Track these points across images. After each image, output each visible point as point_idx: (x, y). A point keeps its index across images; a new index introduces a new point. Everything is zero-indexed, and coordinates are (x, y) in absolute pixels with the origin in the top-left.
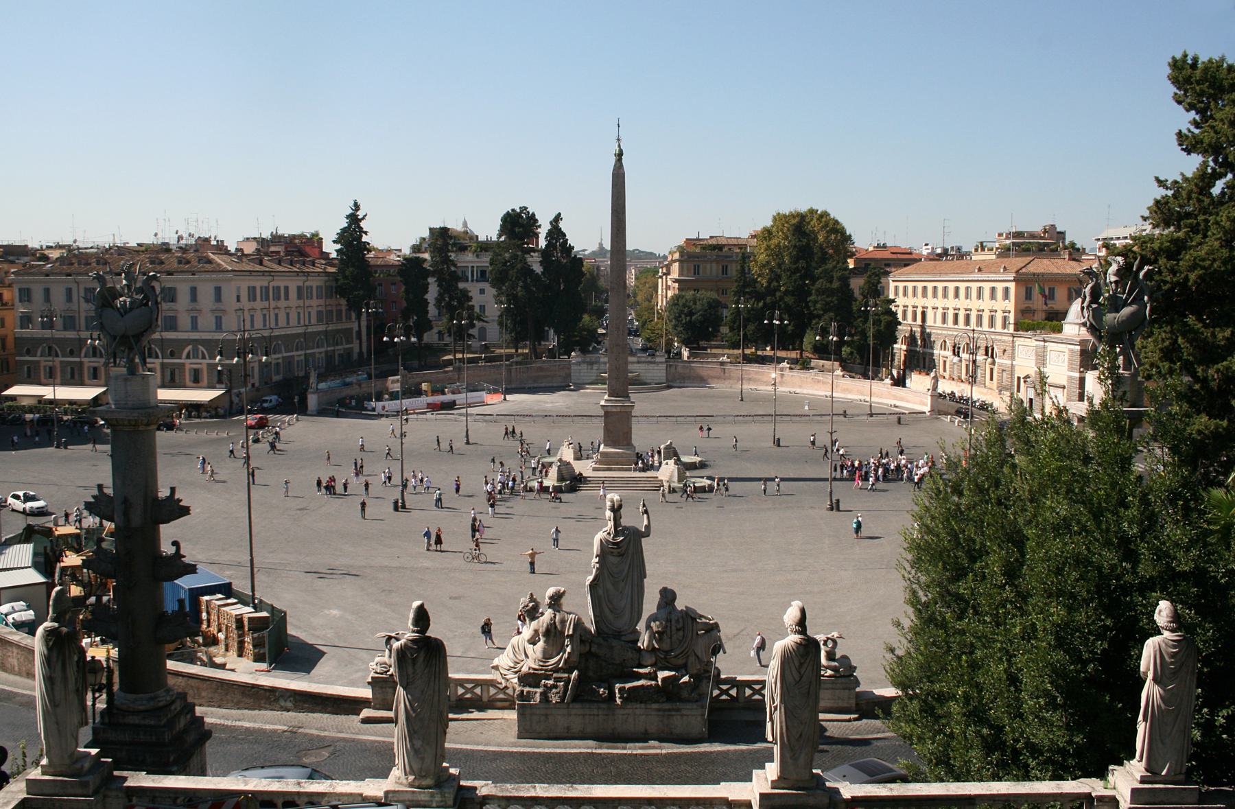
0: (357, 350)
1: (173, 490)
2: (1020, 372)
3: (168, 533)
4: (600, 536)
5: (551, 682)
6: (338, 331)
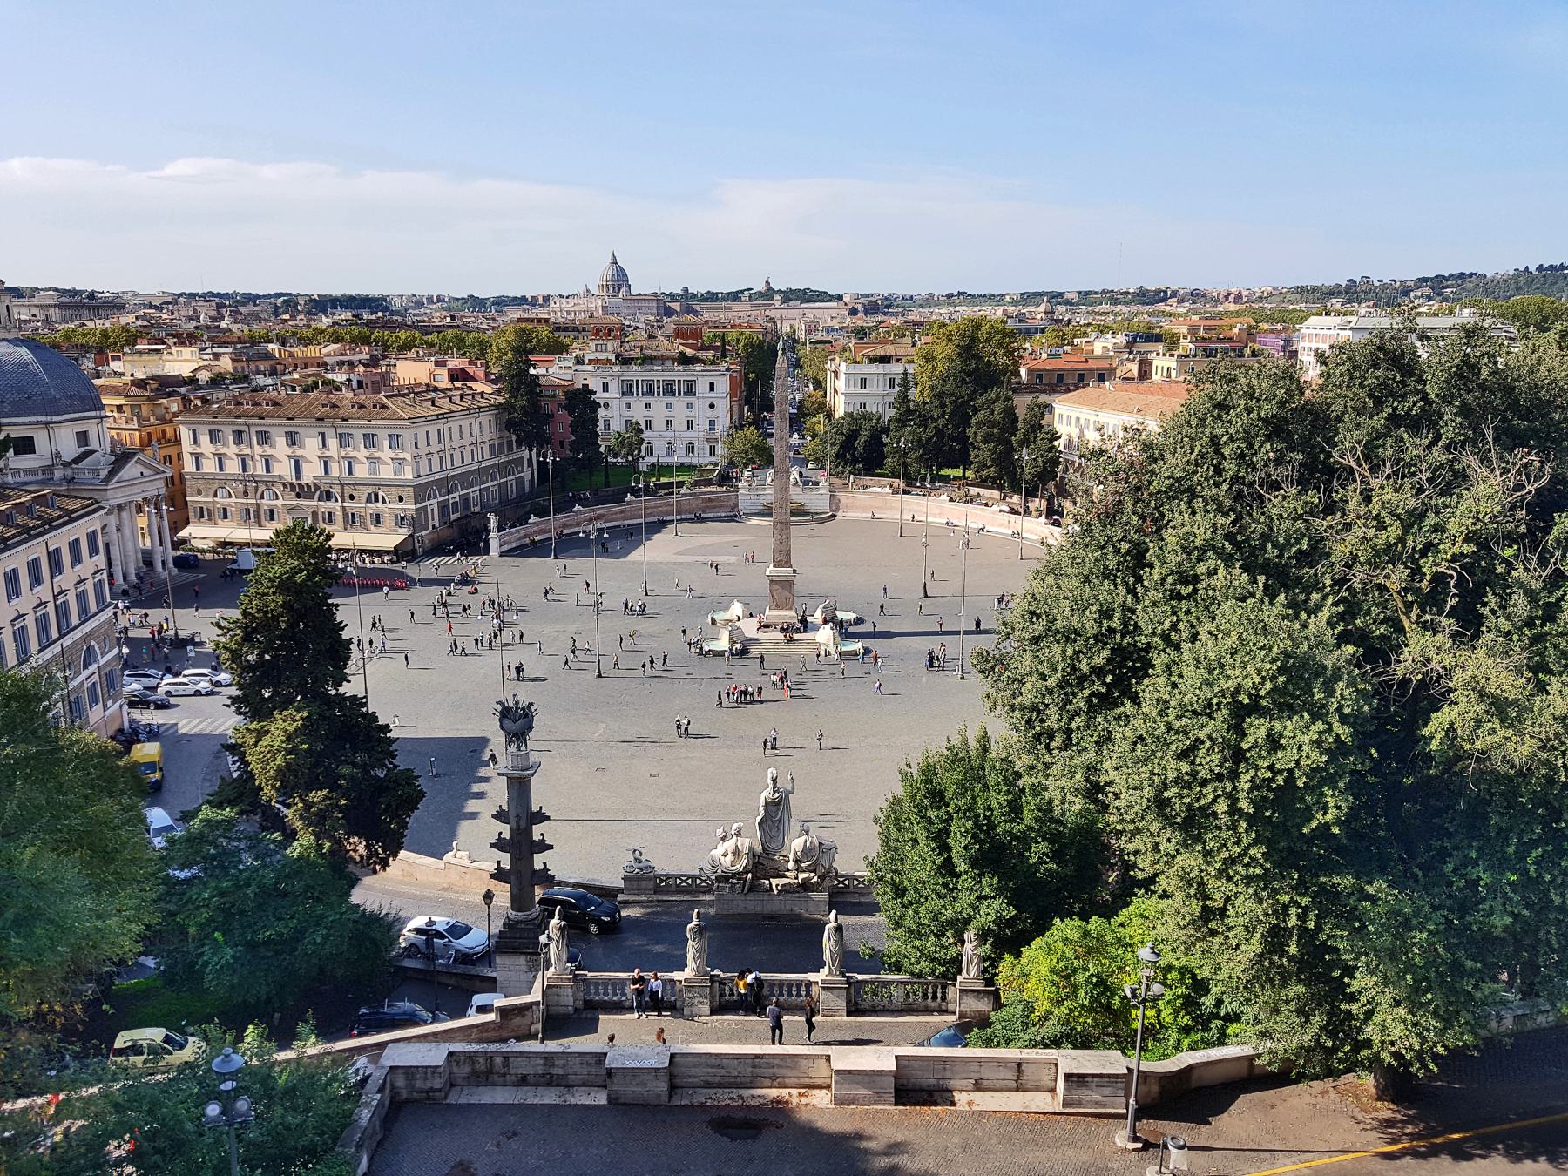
4: (763, 795)
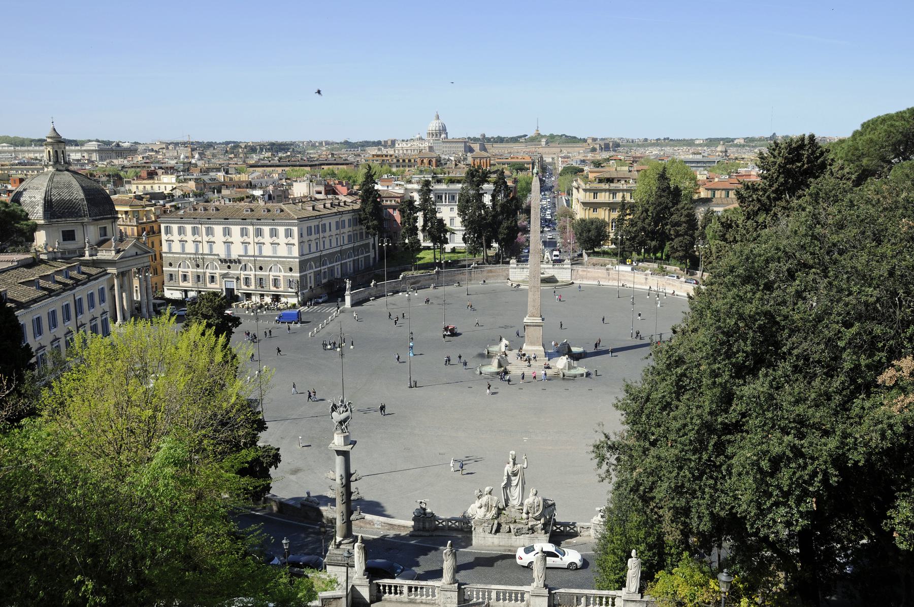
6: (360, 246)
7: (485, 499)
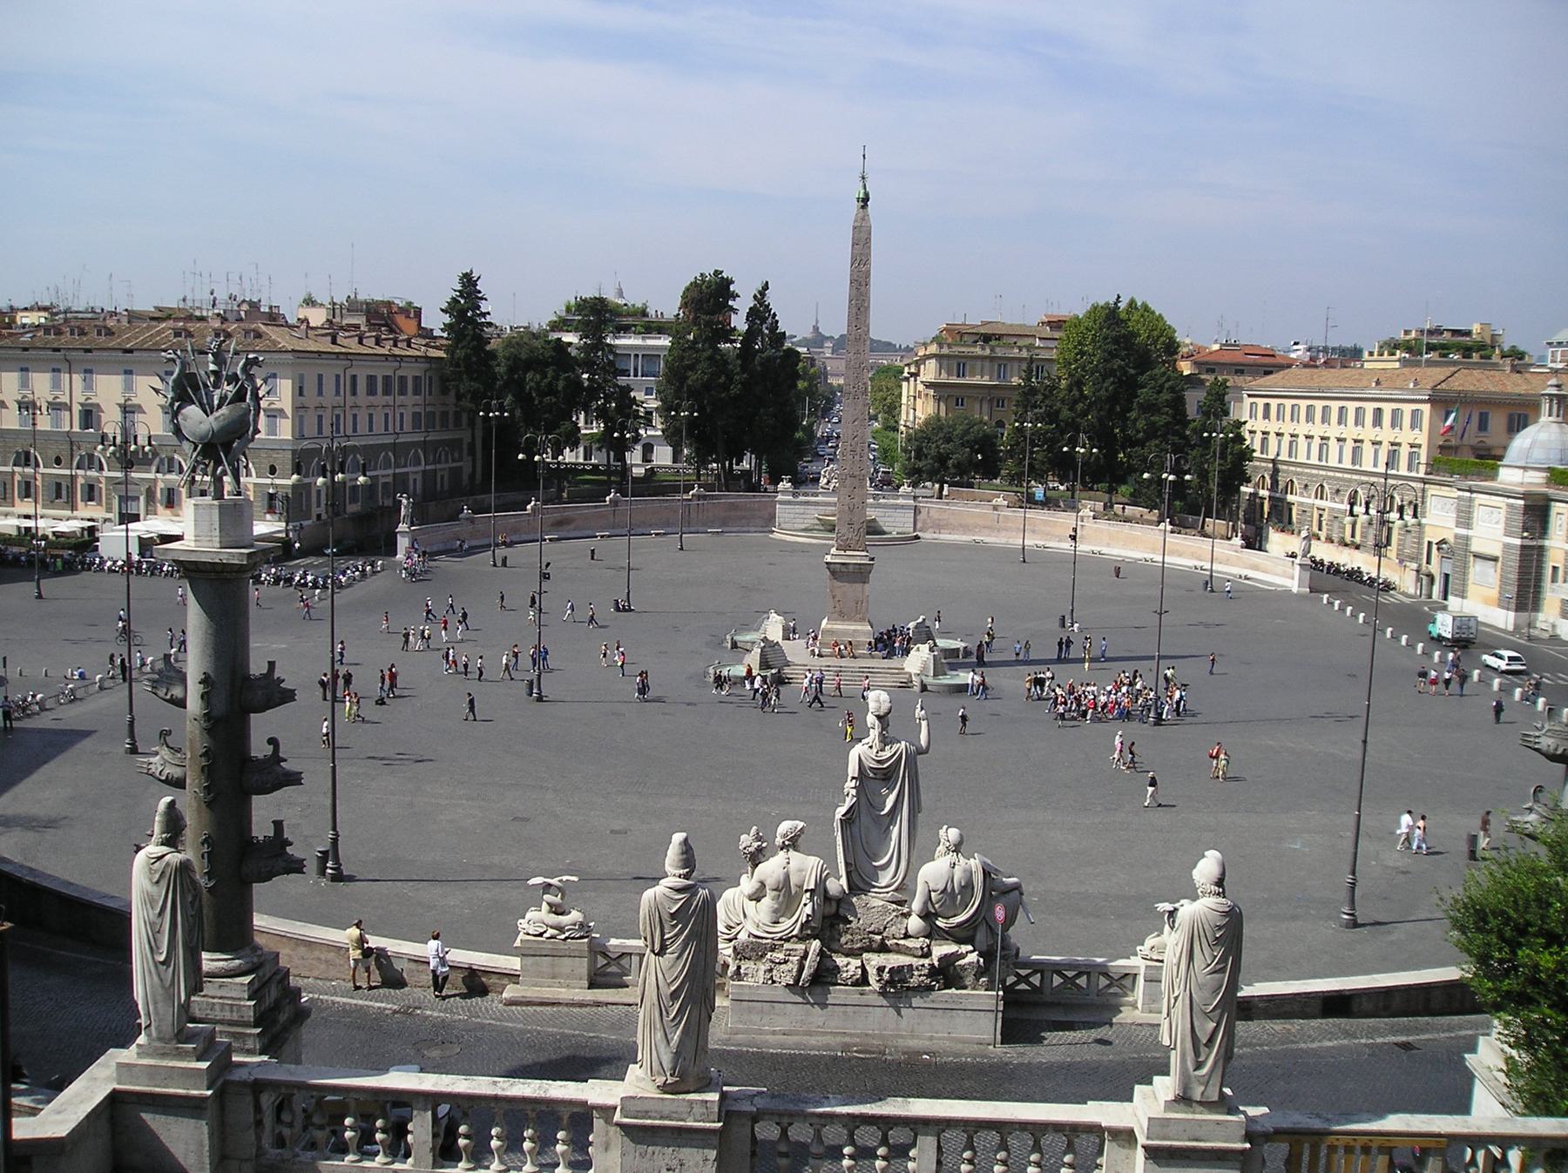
0: (467, 470)
1: (272, 665)
2: (1432, 535)
3: (262, 728)
5: (781, 956)
7: (771, 868)
